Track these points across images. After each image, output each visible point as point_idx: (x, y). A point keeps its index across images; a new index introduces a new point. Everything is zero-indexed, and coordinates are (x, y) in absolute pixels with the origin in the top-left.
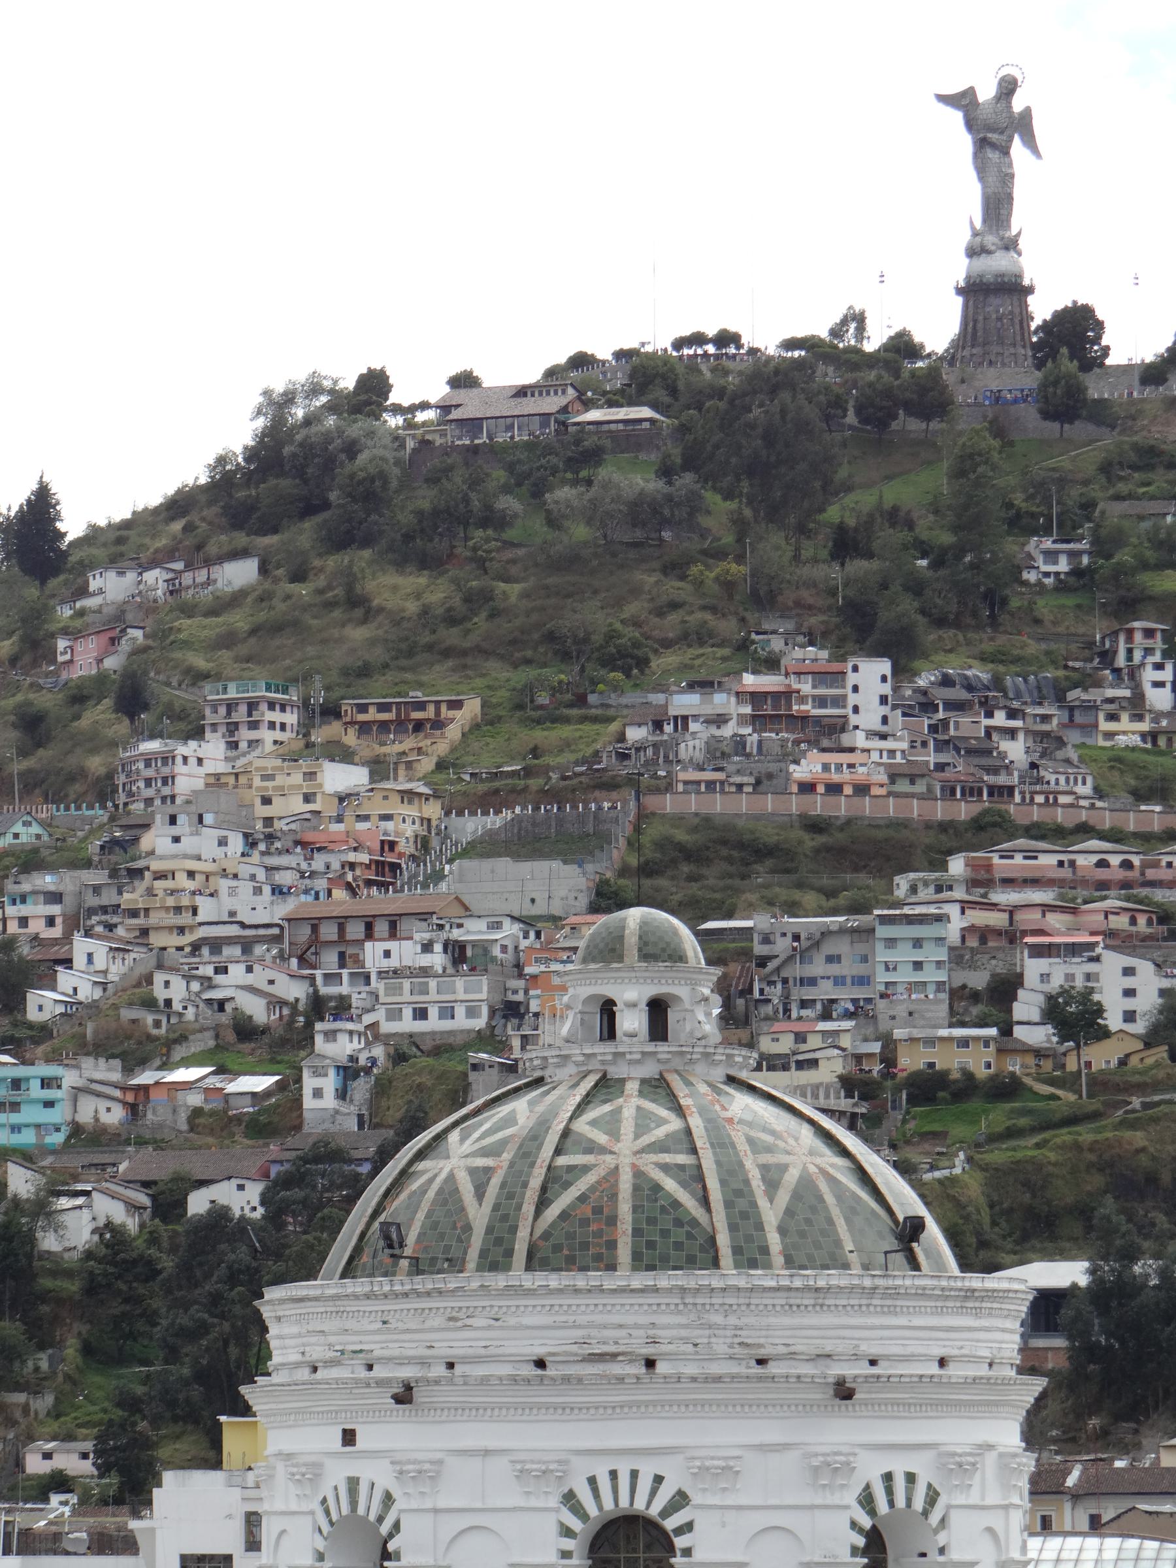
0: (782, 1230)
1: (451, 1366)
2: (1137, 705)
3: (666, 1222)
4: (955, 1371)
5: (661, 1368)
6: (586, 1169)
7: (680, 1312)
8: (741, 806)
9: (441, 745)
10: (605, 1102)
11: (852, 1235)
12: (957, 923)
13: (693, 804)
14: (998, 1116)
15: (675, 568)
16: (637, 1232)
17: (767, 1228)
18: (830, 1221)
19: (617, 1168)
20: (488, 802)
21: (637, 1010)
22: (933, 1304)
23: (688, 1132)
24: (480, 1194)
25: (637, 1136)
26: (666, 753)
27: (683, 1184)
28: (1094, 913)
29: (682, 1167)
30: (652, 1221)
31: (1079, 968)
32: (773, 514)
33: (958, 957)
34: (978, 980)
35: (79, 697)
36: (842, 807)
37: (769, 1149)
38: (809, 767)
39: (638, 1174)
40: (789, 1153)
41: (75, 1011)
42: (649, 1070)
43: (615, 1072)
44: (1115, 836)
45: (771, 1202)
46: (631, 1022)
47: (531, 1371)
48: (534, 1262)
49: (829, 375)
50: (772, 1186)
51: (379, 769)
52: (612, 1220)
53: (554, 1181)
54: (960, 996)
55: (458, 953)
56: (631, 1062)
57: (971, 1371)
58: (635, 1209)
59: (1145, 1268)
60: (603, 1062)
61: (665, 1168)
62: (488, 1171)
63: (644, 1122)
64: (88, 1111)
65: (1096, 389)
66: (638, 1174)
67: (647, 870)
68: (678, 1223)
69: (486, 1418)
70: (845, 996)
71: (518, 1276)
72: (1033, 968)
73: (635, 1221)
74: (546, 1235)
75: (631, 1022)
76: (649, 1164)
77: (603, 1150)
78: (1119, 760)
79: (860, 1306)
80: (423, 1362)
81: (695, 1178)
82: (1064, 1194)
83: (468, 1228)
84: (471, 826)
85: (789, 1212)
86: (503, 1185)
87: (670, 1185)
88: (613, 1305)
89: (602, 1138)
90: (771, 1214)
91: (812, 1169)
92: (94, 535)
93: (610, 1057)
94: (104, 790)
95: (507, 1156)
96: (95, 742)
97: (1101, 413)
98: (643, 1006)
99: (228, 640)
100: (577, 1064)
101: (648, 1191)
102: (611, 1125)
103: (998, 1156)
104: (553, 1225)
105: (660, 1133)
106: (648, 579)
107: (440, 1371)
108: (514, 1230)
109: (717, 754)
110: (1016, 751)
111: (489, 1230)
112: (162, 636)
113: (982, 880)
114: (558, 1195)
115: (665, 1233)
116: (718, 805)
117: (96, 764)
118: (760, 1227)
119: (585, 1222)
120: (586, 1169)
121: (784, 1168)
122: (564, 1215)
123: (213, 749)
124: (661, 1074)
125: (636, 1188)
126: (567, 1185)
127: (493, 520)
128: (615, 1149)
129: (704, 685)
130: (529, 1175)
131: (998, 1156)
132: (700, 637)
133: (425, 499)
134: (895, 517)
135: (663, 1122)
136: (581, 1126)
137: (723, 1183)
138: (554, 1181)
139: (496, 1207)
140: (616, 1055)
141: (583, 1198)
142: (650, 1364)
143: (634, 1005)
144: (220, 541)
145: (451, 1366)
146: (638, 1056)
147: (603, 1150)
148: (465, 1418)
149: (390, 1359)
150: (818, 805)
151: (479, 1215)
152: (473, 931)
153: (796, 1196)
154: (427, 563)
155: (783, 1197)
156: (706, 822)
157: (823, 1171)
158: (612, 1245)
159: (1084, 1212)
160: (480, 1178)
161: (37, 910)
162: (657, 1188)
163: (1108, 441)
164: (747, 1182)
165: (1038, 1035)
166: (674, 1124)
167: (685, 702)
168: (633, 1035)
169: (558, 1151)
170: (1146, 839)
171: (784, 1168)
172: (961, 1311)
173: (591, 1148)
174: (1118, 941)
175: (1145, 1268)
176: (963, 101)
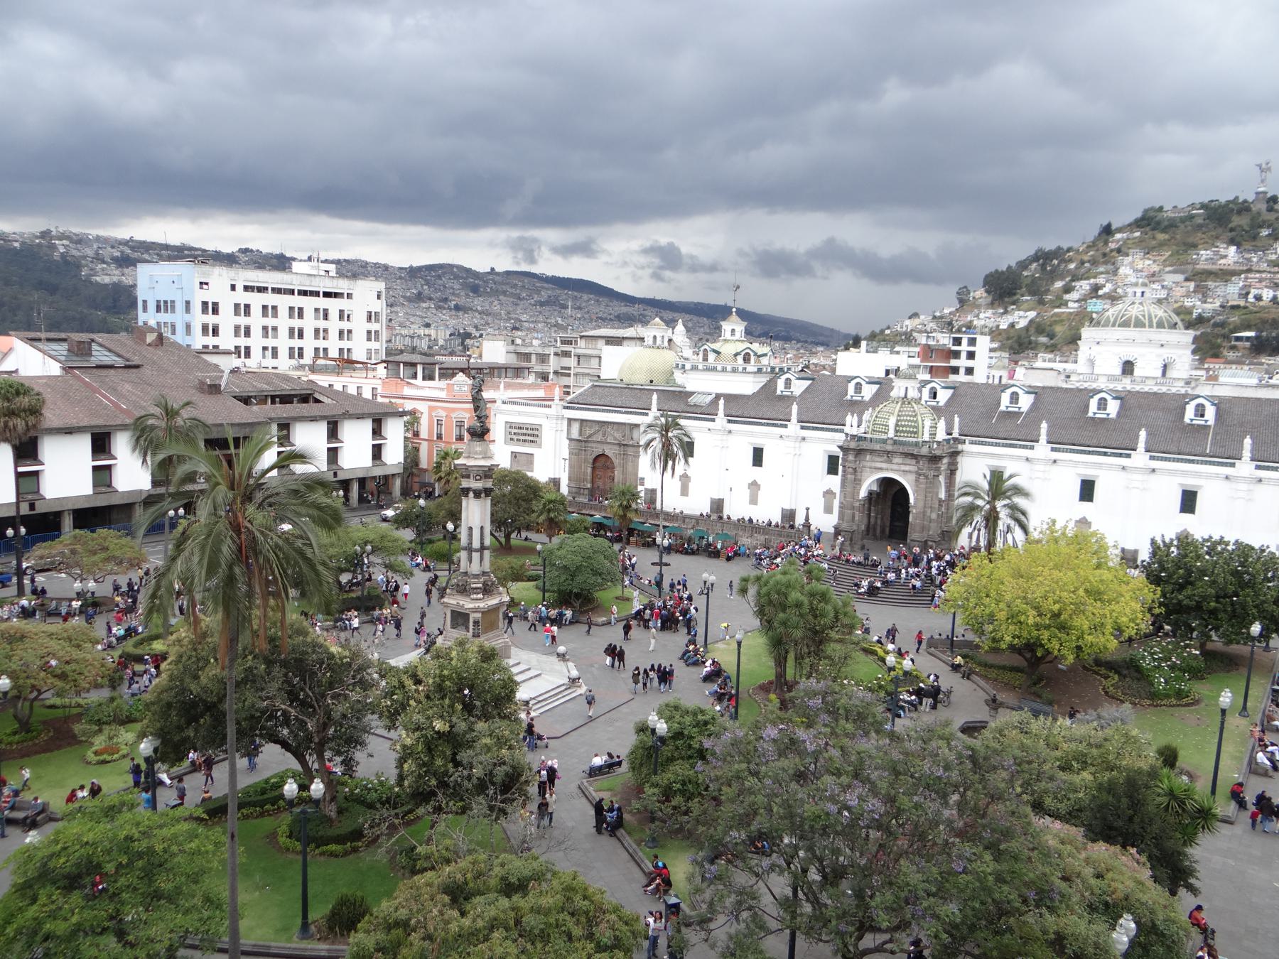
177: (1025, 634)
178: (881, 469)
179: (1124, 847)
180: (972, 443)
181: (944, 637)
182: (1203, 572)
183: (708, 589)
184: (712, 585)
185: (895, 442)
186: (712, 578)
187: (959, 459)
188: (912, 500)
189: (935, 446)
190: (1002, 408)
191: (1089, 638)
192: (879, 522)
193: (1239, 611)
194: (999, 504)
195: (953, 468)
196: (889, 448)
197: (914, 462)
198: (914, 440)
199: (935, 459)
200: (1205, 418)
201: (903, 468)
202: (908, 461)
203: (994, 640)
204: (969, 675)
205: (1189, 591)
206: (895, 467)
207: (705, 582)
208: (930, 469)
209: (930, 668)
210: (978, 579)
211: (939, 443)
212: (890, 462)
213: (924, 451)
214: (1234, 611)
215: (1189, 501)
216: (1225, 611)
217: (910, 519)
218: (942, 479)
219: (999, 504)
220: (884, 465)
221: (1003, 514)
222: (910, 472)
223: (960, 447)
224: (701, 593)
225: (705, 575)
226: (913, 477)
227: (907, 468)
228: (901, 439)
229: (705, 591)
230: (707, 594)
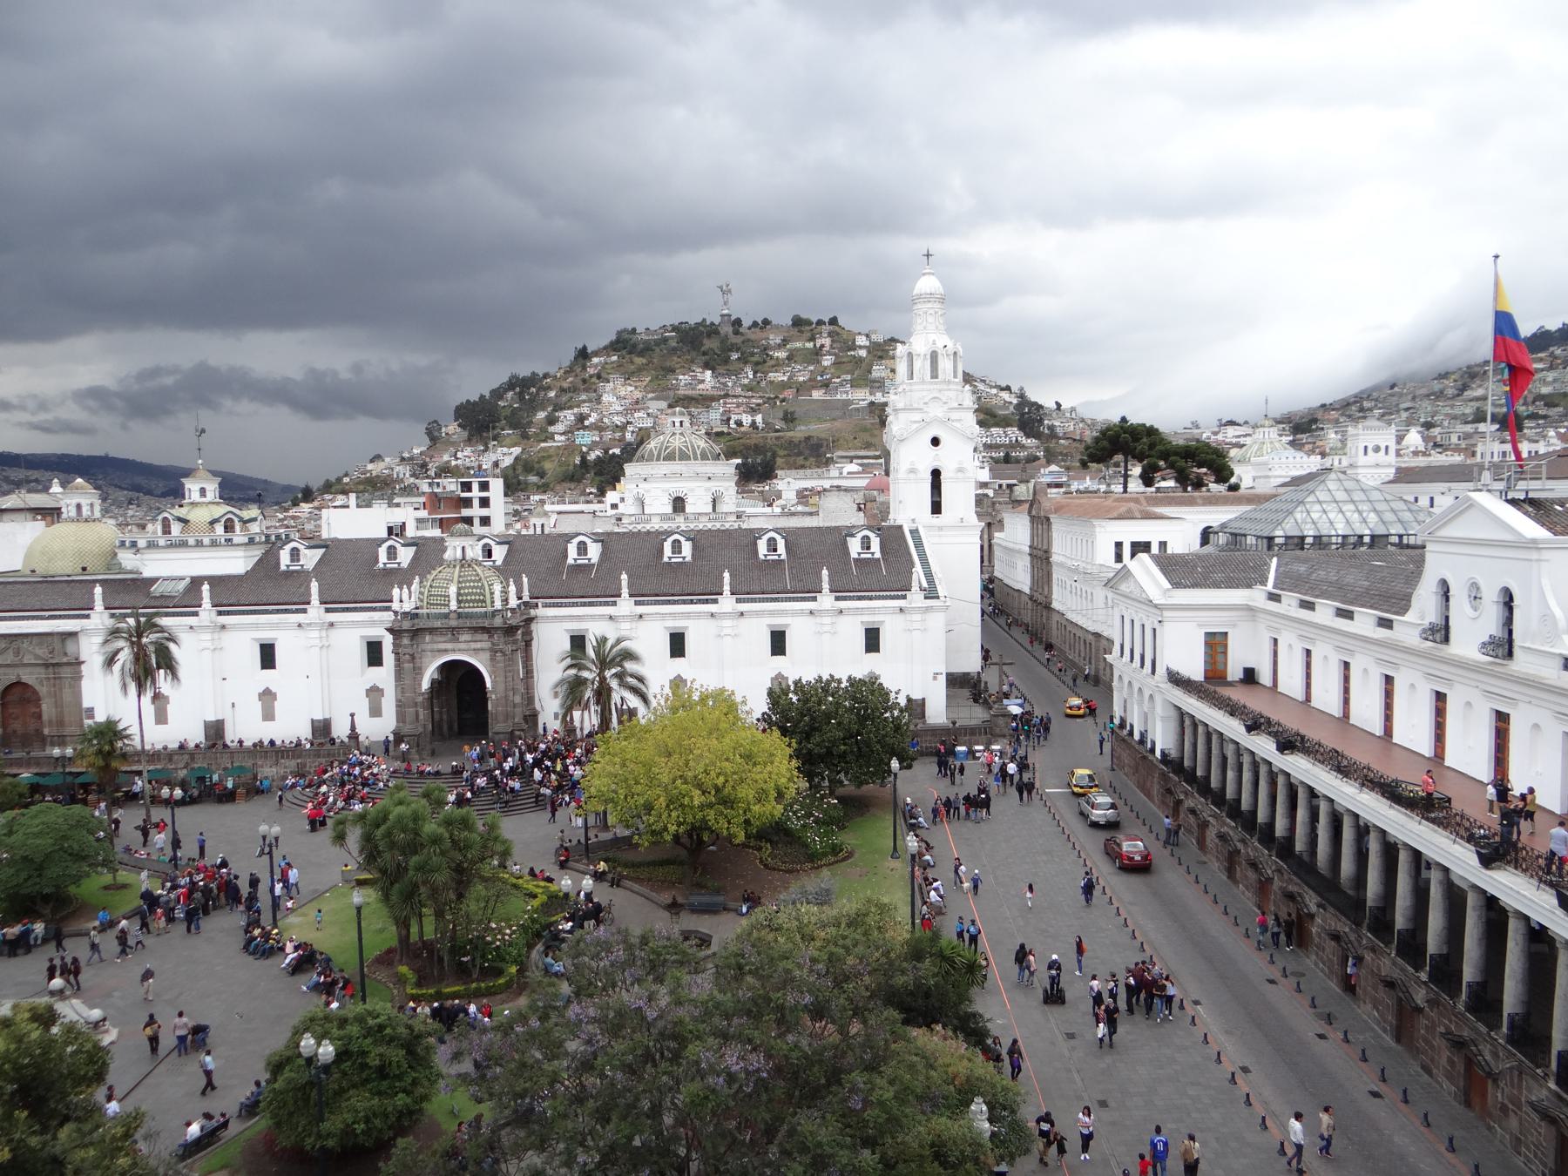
2: (747, 377)
8: (689, 392)
9: (645, 383)
12: (722, 409)
13: (683, 392)
14: (728, 438)
15: (679, 357)
20: (653, 392)
26: (678, 385)
28: (741, 408)
31: (739, 417)
32: (694, 349)
33: (722, 415)
34: (725, 418)
35: (591, 376)
36: (704, 393)
38: (700, 386)
41: (592, 424)
44: (745, 397)
46: (678, 424)
48: (664, 460)
49: (701, 328)
50: (698, 448)
51: (636, 387)
53: (667, 448)
54: (722, 420)
55: (648, 414)
59: (750, 460)
64: (594, 439)
65: (741, 330)
67: (676, 402)
70: (705, 420)
72: (733, 416)
75: (678, 424)
78: (745, 385)
81: (687, 447)
82: (737, 450)
84: (650, 395)
90: (698, 453)
92: (592, 352)
94: (595, 391)
96: (594, 383)
97: (742, 334)
99: (613, 368)
101: (680, 449)
102: (675, 439)
103: (728, 444)
106: (675, 358)
109: (686, 385)
110: (730, 384)
112: (603, 367)
113: (725, 403)
116: (686, 393)
117: (594, 387)
123: (611, 384)
127: (652, 350)
129: (684, 375)
131: (728, 444)
132: (684, 367)
133: (641, 346)
134: (712, 349)
138: (667, 448)
144: (611, 353)
150: (701, 392)
151: (656, 453)
152: (651, 411)
154: (643, 356)
156: (684, 395)
159: (741, 452)
160: (656, 447)
161: (586, 409)
163: (742, 338)
165: (733, 426)
167: (681, 377)
170: (749, 397)
174: (744, 412)
175: (750, 460)
176: (721, 288)
177: (690, 819)
178: (446, 651)
179: (929, 1026)
180: (546, 606)
181: (575, 842)
182: (828, 716)
183: (270, 846)
184: (277, 839)
185: (460, 616)
186: (276, 830)
187: (533, 626)
188: (489, 685)
189: (509, 614)
190: (570, 561)
191: (756, 808)
192: (445, 717)
193: (865, 749)
194: (608, 674)
195: (528, 639)
196: (453, 623)
197: (486, 636)
198: (485, 609)
199: (510, 630)
200: (872, 551)
201: (474, 645)
202: (479, 636)
203: (653, 833)
204: (619, 880)
205: (817, 738)
206: (463, 646)
207: (264, 838)
208: (506, 643)
209: (578, 884)
210: (624, 765)
211: (513, 610)
212: (457, 640)
213: (498, 622)
214: (859, 749)
215: (778, 643)
216: (852, 752)
217: (490, 708)
218: (519, 655)
219: (608, 674)
220: (449, 646)
221: (614, 684)
222: (482, 649)
223: (533, 612)
224: (262, 853)
225: (263, 828)
226: (487, 655)
227: (479, 645)
228: (466, 610)
229: (267, 850)
230: (270, 853)
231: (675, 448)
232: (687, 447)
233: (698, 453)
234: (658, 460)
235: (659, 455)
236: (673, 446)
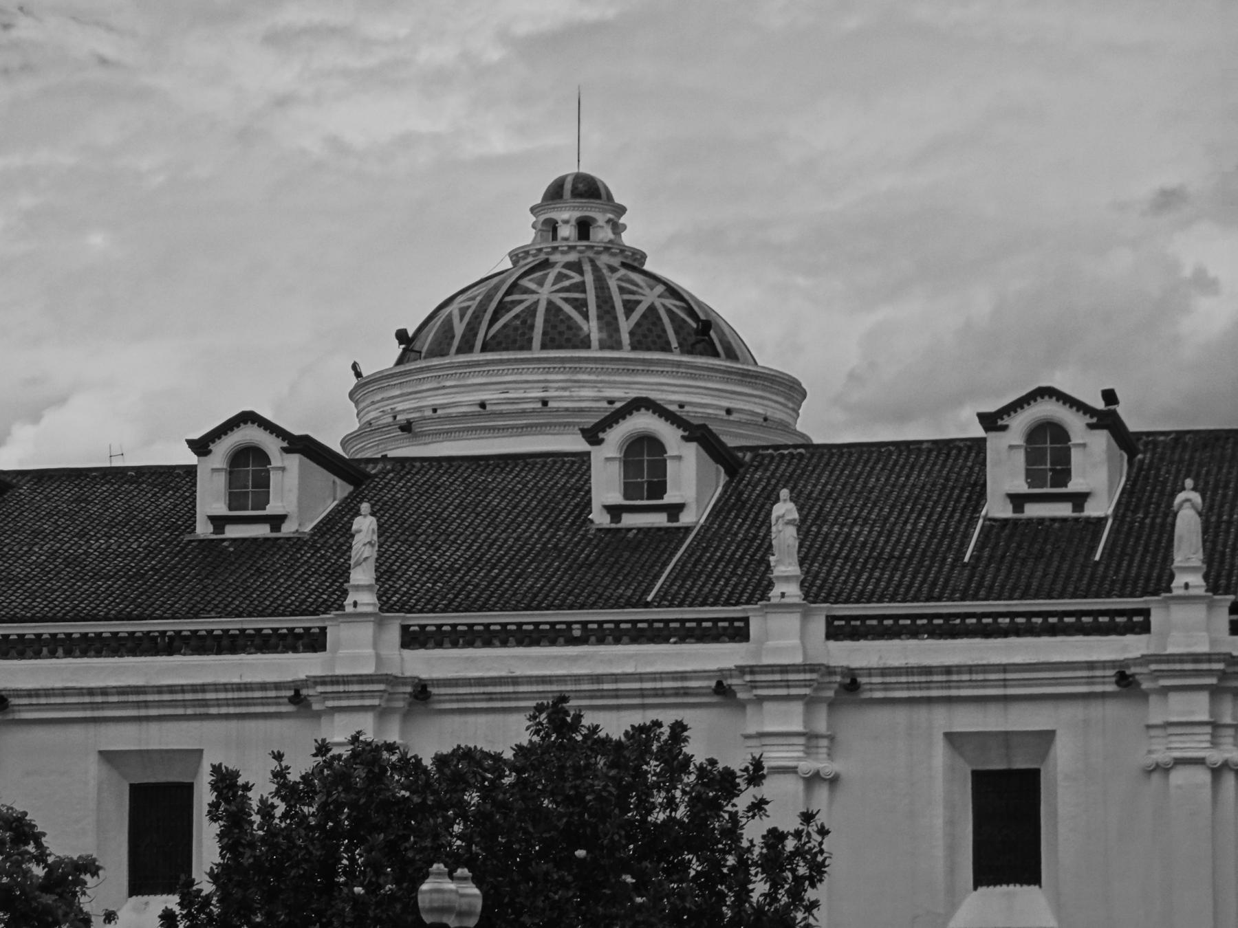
0: (632, 333)
1: (435, 411)
3: (562, 328)
4: (734, 417)
5: (551, 404)
6: (521, 302)
7: (562, 373)
10: (541, 271)
11: (678, 339)
16: (545, 333)
17: (621, 330)
18: (664, 331)
19: (538, 300)
21: (568, 226)
22: (721, 375)
23: (583, 282)
24: (461, 319)
25: (553, 284)
27: (575, 308)
29: (576, 300)
30: (554, 327)
37: (633, 293)
39: (550, 303)
40: (643, 295)
42: (572, 257)
43: (553, 258)
45: (627, 318)
46: (566, 231)
47: (478, 409)
50: (630, 307)
52: (532, 327)
53: (502, 308)
56: (563, 253)
57: (744, 417)
58: (546, 321)
60: (548, 253)
61: (566, 300)
62: (469, 307)
63: (560, 277)
66: (550, 303)
68: (569, 328)
69: (452, 438)
71: (477, 356)
73: (544, 327)
74: (494, 337)
75: (566, 231)
76: (557, 299)
77: (533, 292)
79: (673, 372)
80: (419, 409)
81: (581, 306)
83: (453, 337)
85: (638, 324)
86: (474, 313)
87: (567, 308)
88: (523, 369)
89: (533, 286)
90: (625, 326)
91: (658, 304)
93: (549, 250)
95: (479, 298)
98: (573, 222)
100: (534, 255)
101: (552, 308)
102: (541, 283)
104: (498, 332)
105: (567, 283)
107: (429, 413)
108: (476, 335)
111: (463, 336)
114: (503, 316)
115: (561, 333)
118: (617, 330)
119: (516, 329)
120: (521, 302)
121: (638, 302)
122: (505, 326)
124: (579, 258)
125: (547, 310)
126: (509, 310)
128: (540, 291)
130: (488, 305)
135: (572, 278)
136: (526, 282)
137: (599, 307)
138: (502, 308)
139: (468, 324)
140: (555, 249)
141: (517, 317)
142: (545, 403)
143: (566, 222)
145: (435, 411)
146: (566, 248)
147: (533, 292)
148: (441, 439)
149: (404, 411)
151: (459, 329)
153: (644, 316)
155: (636, 316)
157: (664, 306)
158: (530, 340)
160: (463, 312)
162: (559, 309)
164: (613, 307)
166: (577, 278)
168: (566, 239)
169: (508, 293)
171: (638, 302)
172: (741, 383)
173: (527, 291)
231: (532, 311)
232: (581, 306)
233: (625, 326)
234: (466, 346)
235: (471, 330)
236: (530, 299)
